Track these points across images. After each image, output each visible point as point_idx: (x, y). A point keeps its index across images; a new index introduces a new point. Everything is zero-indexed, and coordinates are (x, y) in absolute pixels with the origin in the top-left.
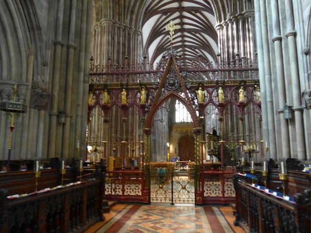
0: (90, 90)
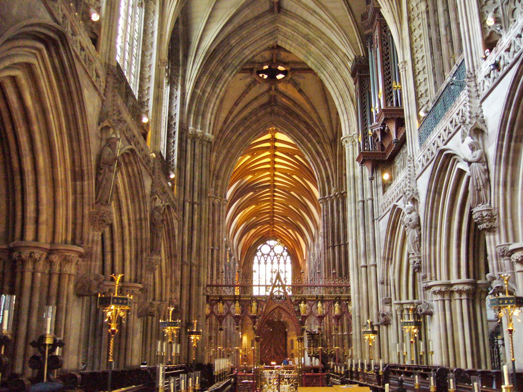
0: (207, 301)
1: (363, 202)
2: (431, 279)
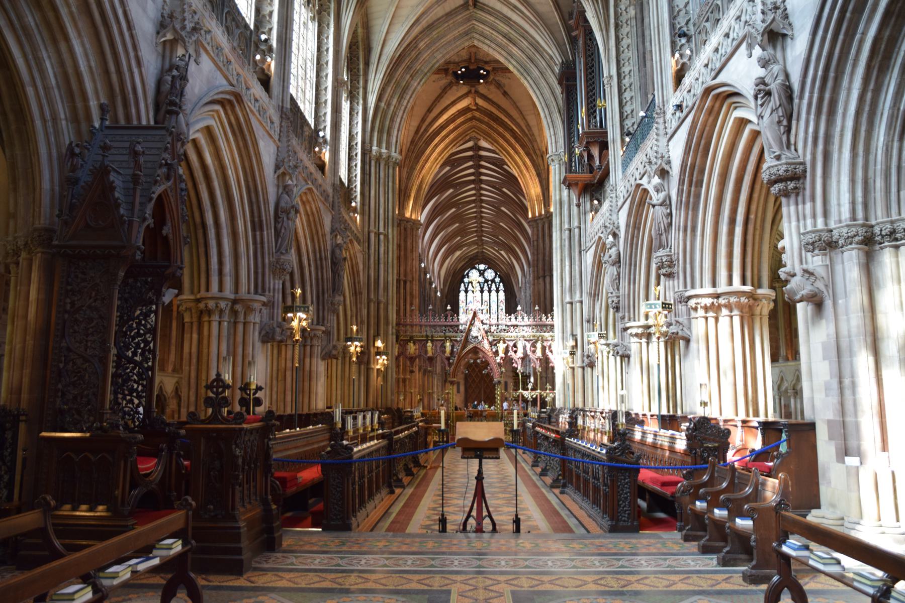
0: (397, 341)
1: (570, 230)
2: (629, 320)
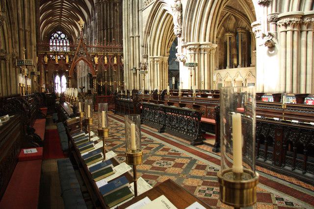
0: (37, 55)
2: (187, 41)
